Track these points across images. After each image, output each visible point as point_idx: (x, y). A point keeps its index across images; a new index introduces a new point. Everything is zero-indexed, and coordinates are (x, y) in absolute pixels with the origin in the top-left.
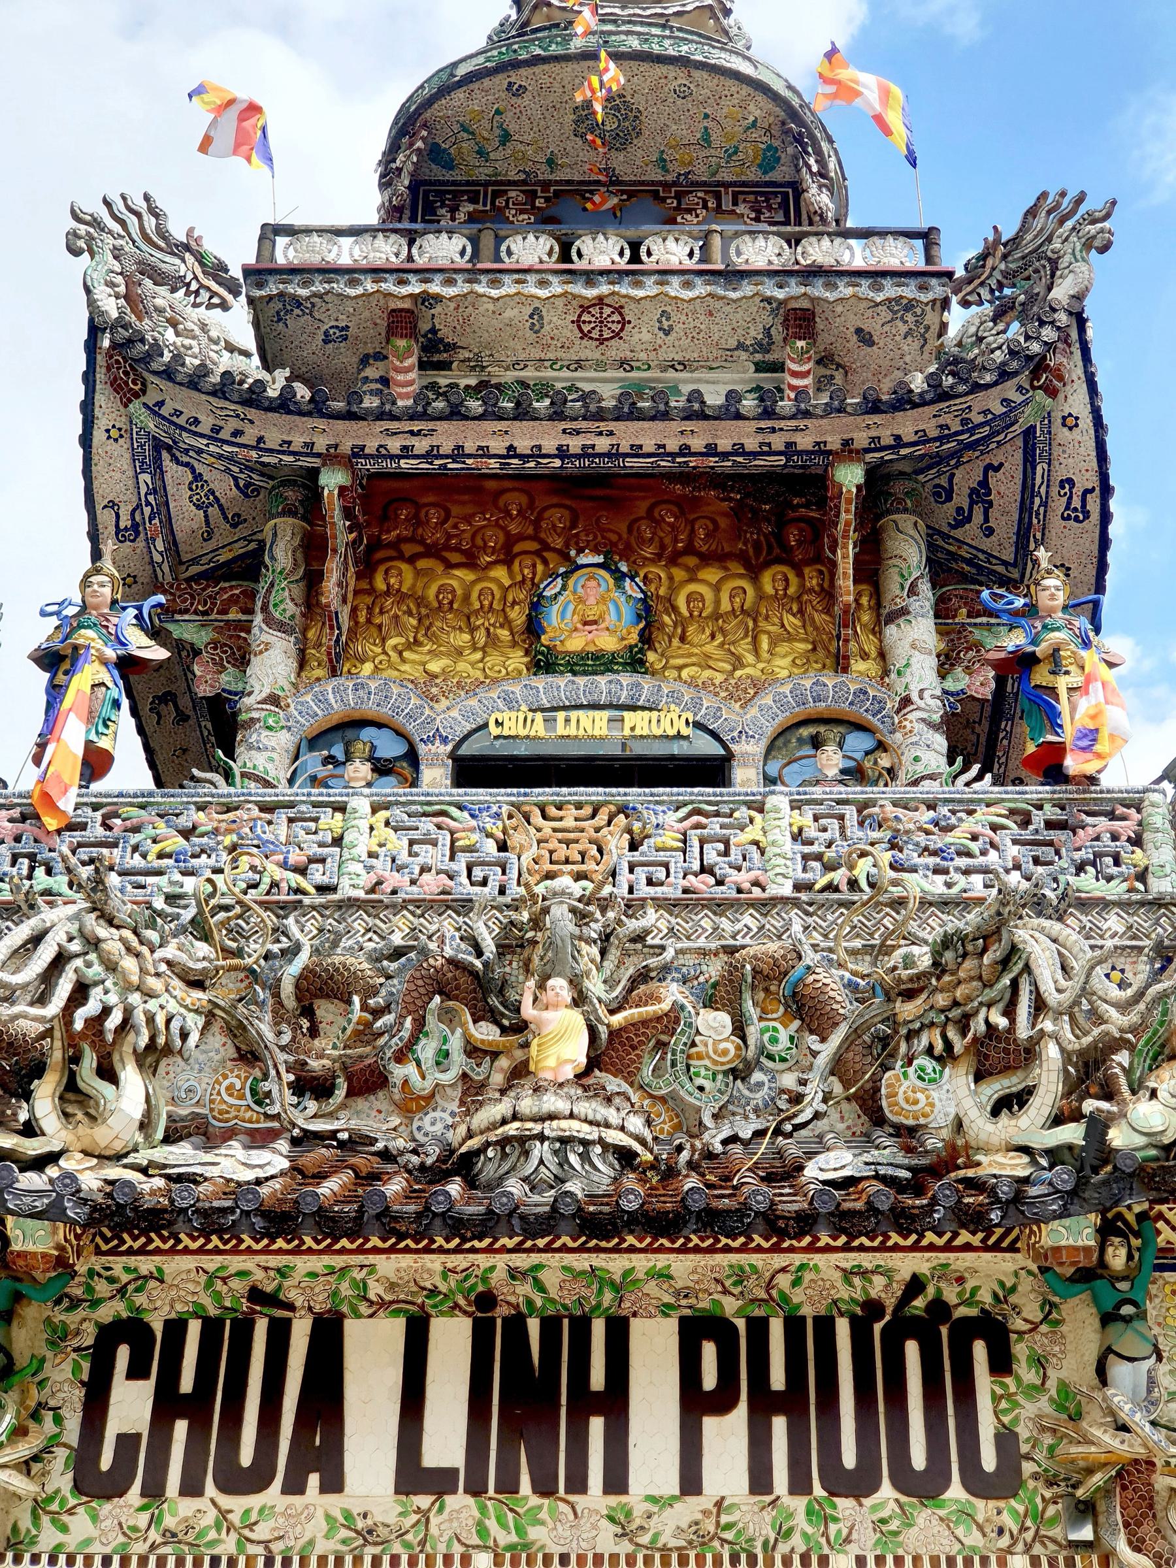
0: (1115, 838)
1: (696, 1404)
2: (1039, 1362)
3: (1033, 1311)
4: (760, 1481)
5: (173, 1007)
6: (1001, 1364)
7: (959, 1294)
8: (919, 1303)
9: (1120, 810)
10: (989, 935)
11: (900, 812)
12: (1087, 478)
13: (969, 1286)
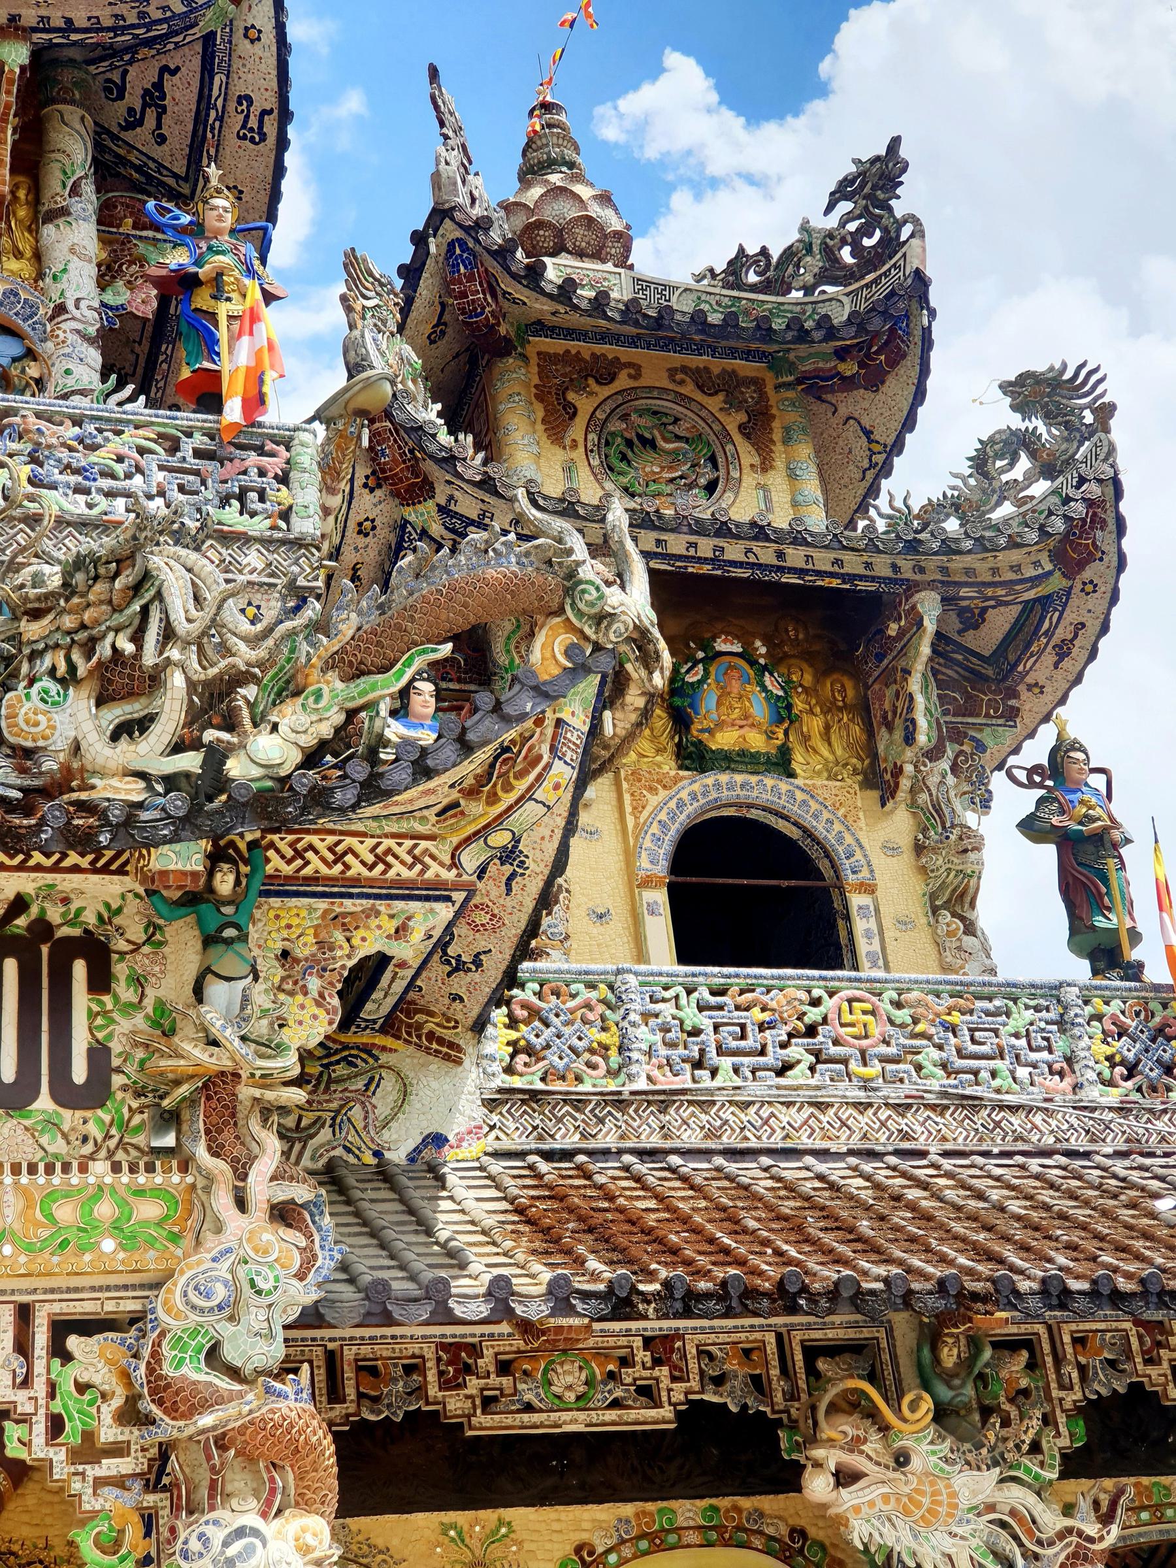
0: (262, 473)
2: (138, 981)
3: (136, 932)
6: (100, 982)
7: (63, 915)
8: (22, 921)
9: (269, 446)
10: (121, 561)
11: (43, 425)
12: (265, 99)
13: (74, 907)
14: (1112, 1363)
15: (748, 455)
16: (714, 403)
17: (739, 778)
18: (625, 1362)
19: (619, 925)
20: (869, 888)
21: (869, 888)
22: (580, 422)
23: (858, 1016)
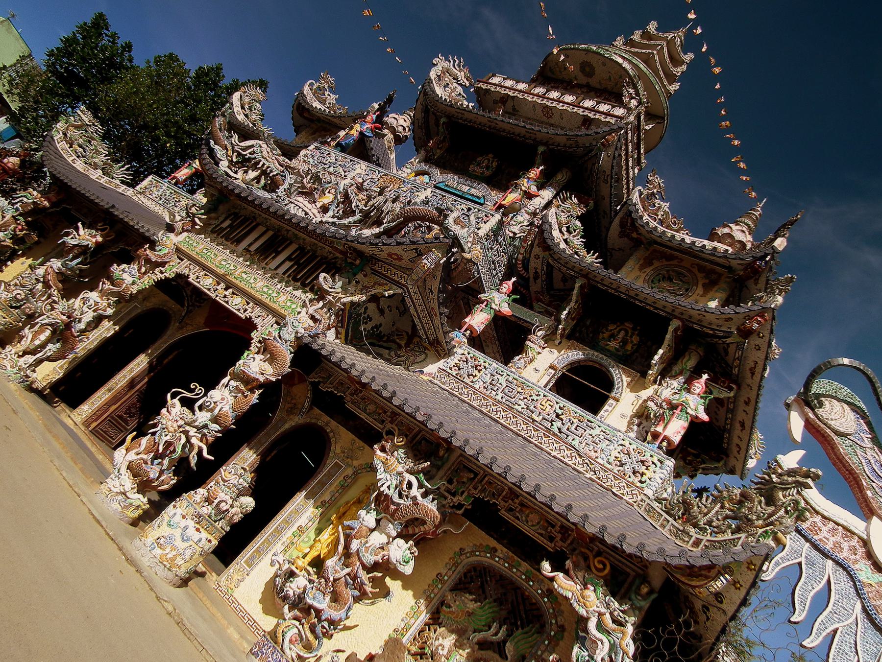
1: (289, 259)
4: (284, 273)
5: (272, 166)
14: (494, 494)
15: (700, 290)
16: (700, 275)
17: (601, 356)
18: (385, 412)
19: (539, 375)
20: (617, 400)
21: (617, 400)
22: (652, 268)
23: (547, 405)
